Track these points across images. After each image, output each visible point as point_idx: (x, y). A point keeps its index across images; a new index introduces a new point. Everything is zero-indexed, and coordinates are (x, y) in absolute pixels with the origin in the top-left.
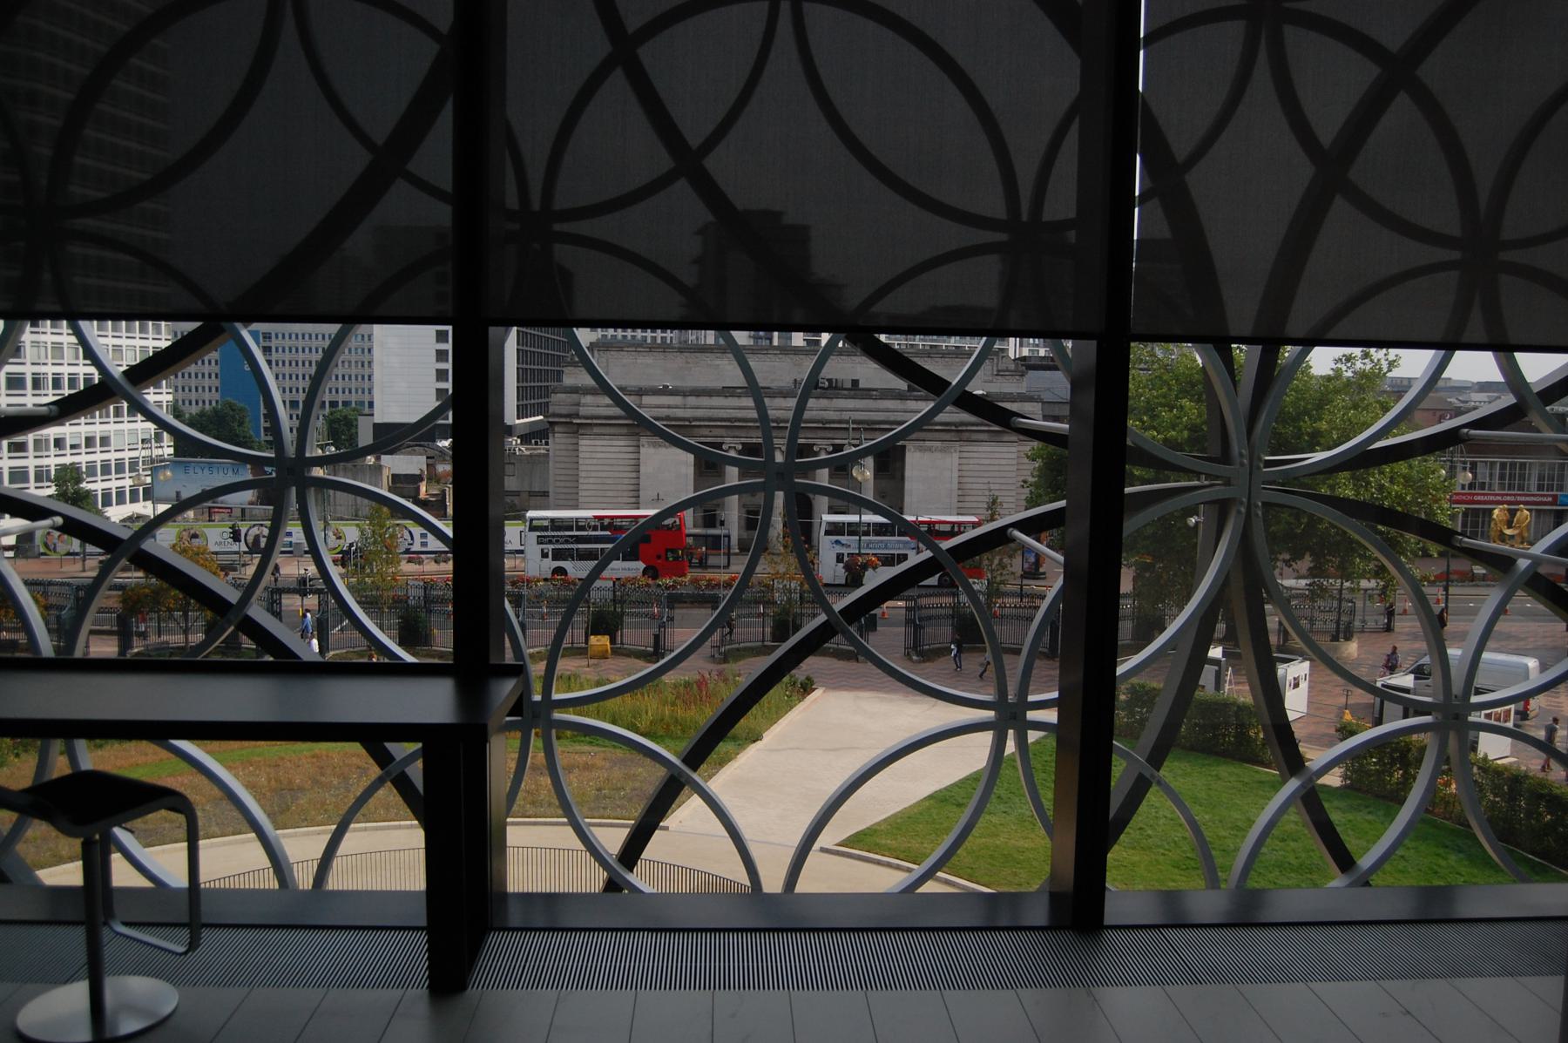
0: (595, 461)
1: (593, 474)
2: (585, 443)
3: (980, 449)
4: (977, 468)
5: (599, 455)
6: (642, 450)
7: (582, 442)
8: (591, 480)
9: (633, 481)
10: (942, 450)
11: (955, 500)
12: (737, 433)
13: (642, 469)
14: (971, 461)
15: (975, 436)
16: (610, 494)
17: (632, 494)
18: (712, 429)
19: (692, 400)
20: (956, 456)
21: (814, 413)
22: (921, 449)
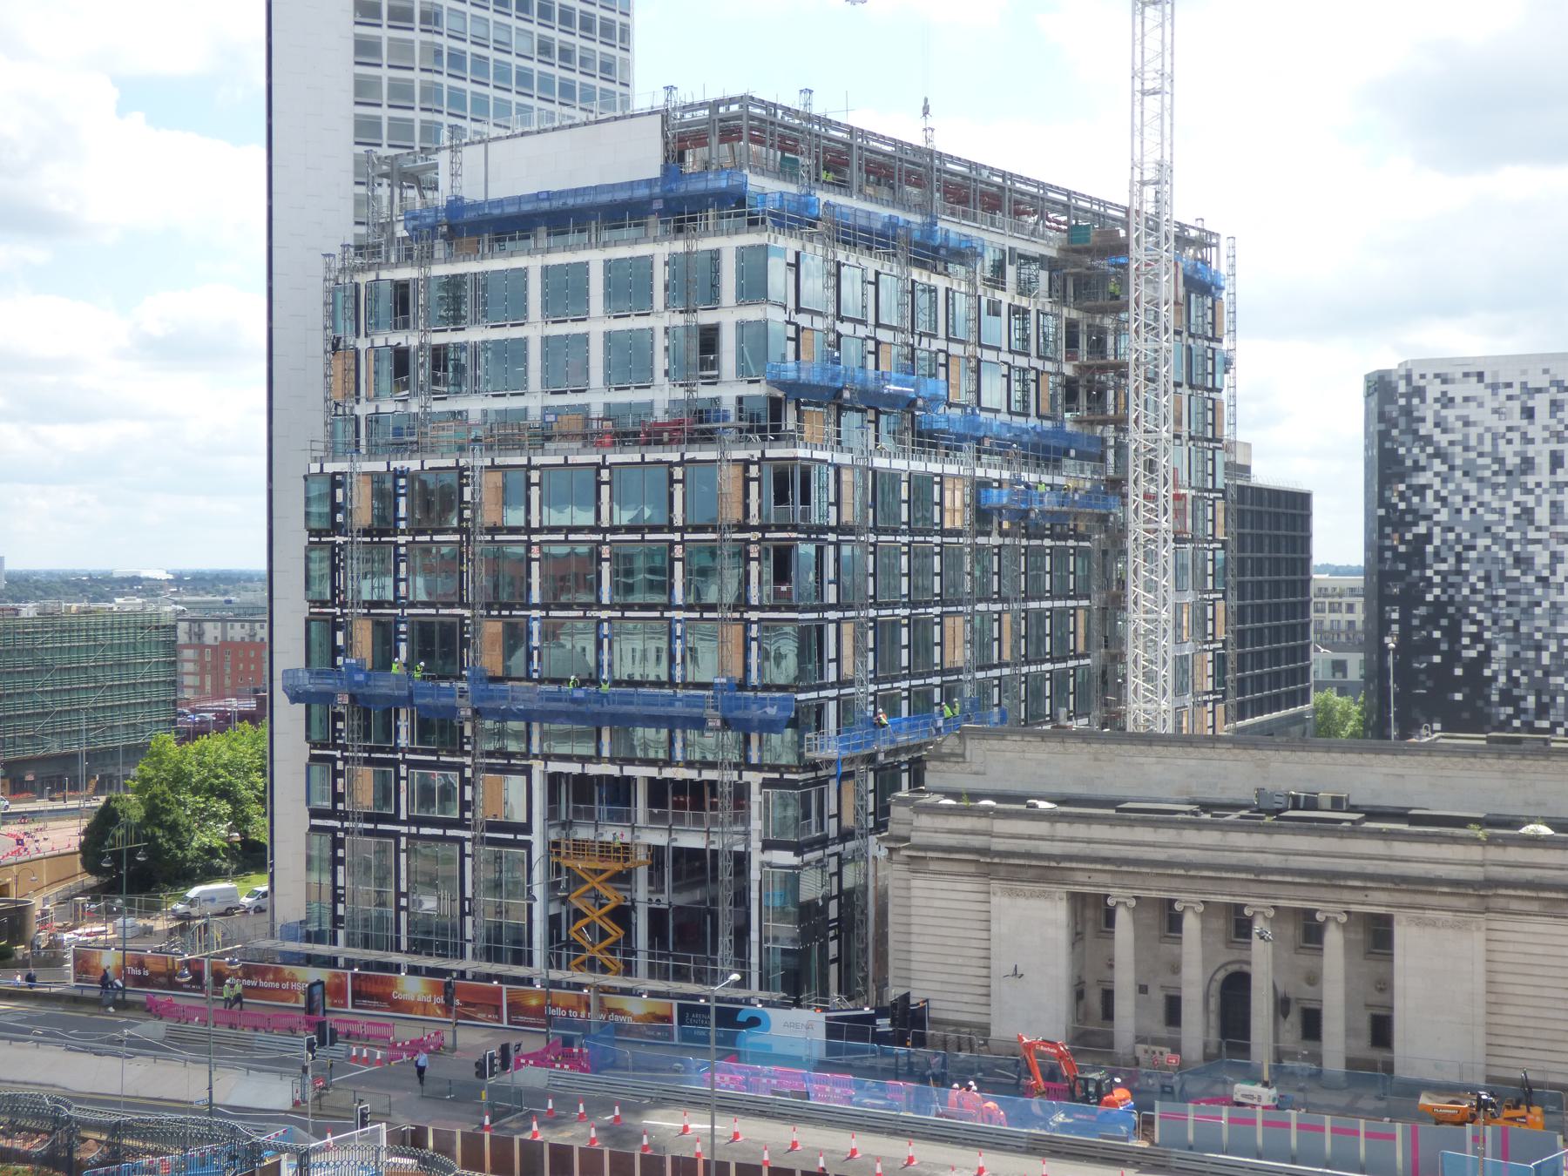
0: (931, 912)
1: (931, 930)
2: (920, 885)
3: (1526, 927)
4: (1522, 959)
5: (937, 903)
6: (994, 900)
7: (915, 883)
8: (927, 939)
9: (984, 944)
10: (1455, 926)
11: (1481, 1011)
12: (1128, 881)
13: (994, 927)
14: (1511, 947)
15: (1515, 905)
16: (952, 960)
17: (983, 962)
18: (1094, 874)
19: (1062, 829)
20: (1480, 937)
21: (1245, 855)
22: (1420, 923)
